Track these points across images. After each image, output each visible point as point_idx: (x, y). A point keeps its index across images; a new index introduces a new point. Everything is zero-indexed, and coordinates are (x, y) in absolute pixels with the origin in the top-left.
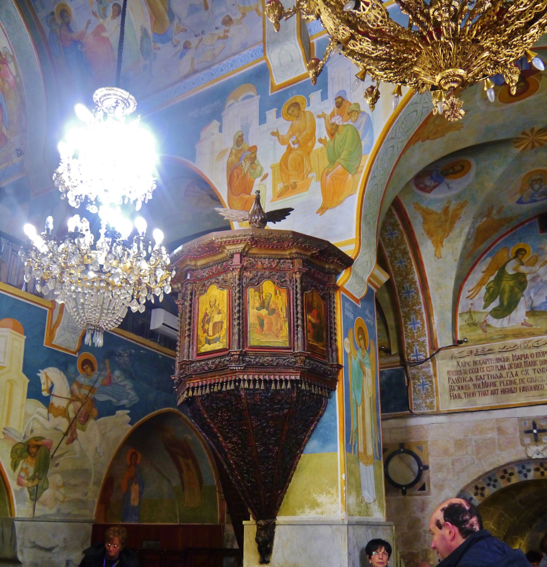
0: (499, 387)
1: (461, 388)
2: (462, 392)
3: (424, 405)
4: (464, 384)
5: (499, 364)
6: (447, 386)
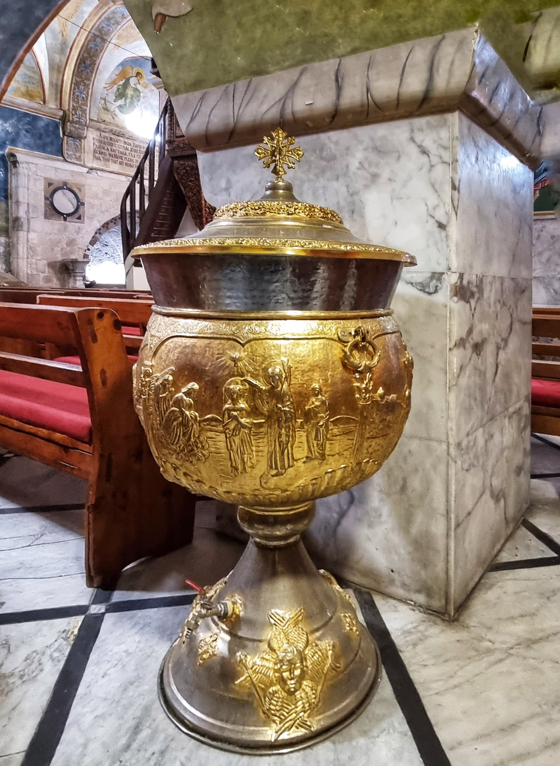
0: (124, 161)
1: (101, 153)
2: (101, 156)
3: (74, 156)
4: (103, 151)
5: (125, 146)
6: (92, 148)
